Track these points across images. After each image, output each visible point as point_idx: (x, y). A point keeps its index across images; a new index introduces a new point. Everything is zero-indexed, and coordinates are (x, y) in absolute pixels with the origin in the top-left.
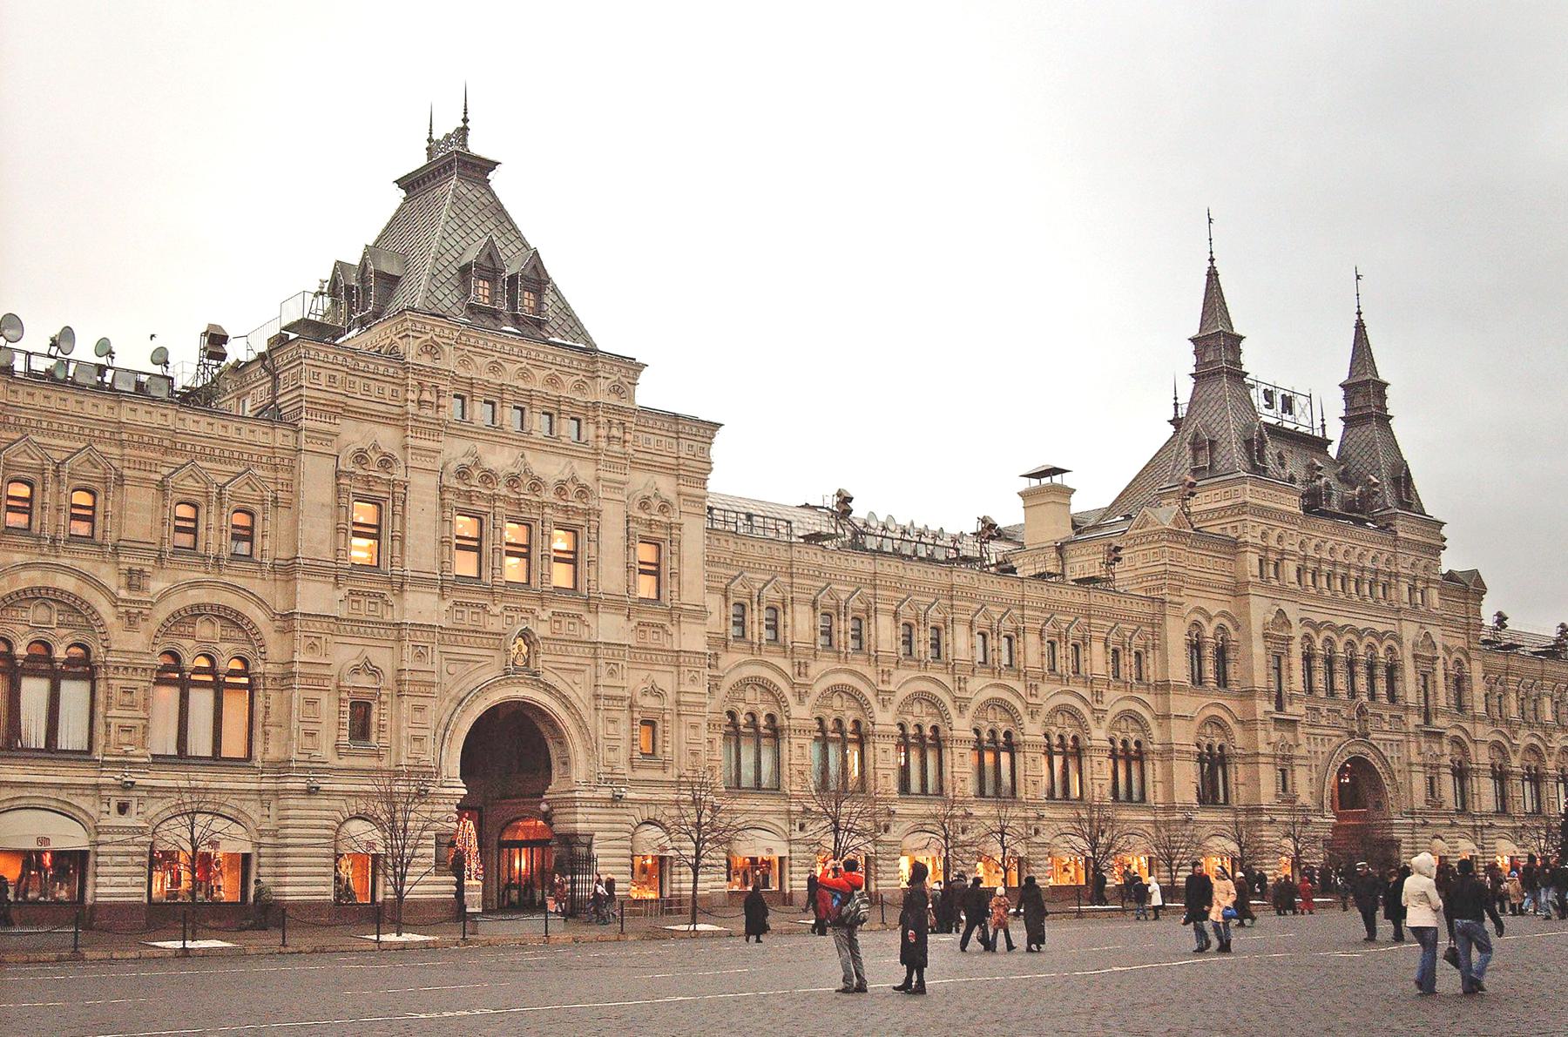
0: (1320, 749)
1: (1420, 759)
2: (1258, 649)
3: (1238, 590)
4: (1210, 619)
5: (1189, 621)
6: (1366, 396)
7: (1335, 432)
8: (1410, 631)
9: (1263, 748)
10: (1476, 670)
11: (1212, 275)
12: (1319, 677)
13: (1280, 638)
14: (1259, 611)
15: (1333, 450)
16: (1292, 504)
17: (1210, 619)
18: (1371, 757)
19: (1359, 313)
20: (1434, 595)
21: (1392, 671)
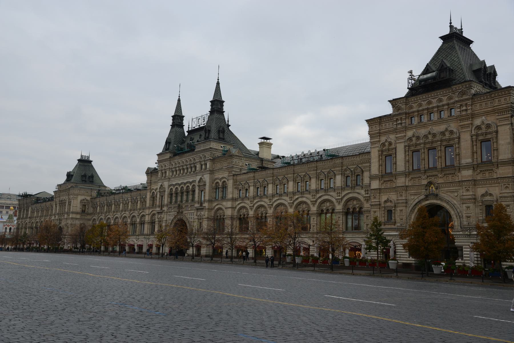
1: (196, 217)
6: (217, 105)
8: (198, 178)
11: (179, 100)
12: (174, 198)
19: (218, 79)
21: (194, 191)
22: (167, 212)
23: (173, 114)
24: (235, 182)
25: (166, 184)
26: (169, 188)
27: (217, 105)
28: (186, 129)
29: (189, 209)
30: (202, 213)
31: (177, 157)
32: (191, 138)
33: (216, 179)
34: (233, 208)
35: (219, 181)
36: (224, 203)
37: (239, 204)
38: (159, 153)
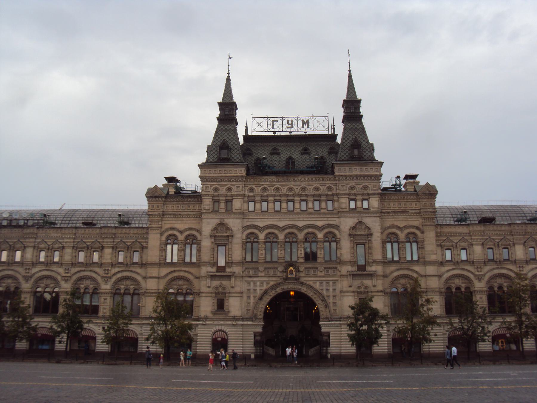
0: (258, 289)
2: (206, 243)
3: (199, 216)
4: (181, 232)
5: (166, 234)
6: (352, 108)
7: (339, 130)
9: (204, 289)
10: (430, 237)
13: (225, 237)
14: (208, 225)
15: (339, 140)
16: (241, 172)
17: (181, 232)
18: (304, 290)
20: (375, 202)
22: (242, 277)
23: (220, 100)
24: (438, 235)
25: (235, 224)
26: (243, 231)
27: (352, 108)
28: (241, 132)
29: (320, 274)
30: (368, 282)
31: (273, 178)
32: (275, 149)
33: (390, 227)
34: (440, 276)
35: (398, 232)
36: (417, 268)
37: (448, 271)
38: (201, 163)
